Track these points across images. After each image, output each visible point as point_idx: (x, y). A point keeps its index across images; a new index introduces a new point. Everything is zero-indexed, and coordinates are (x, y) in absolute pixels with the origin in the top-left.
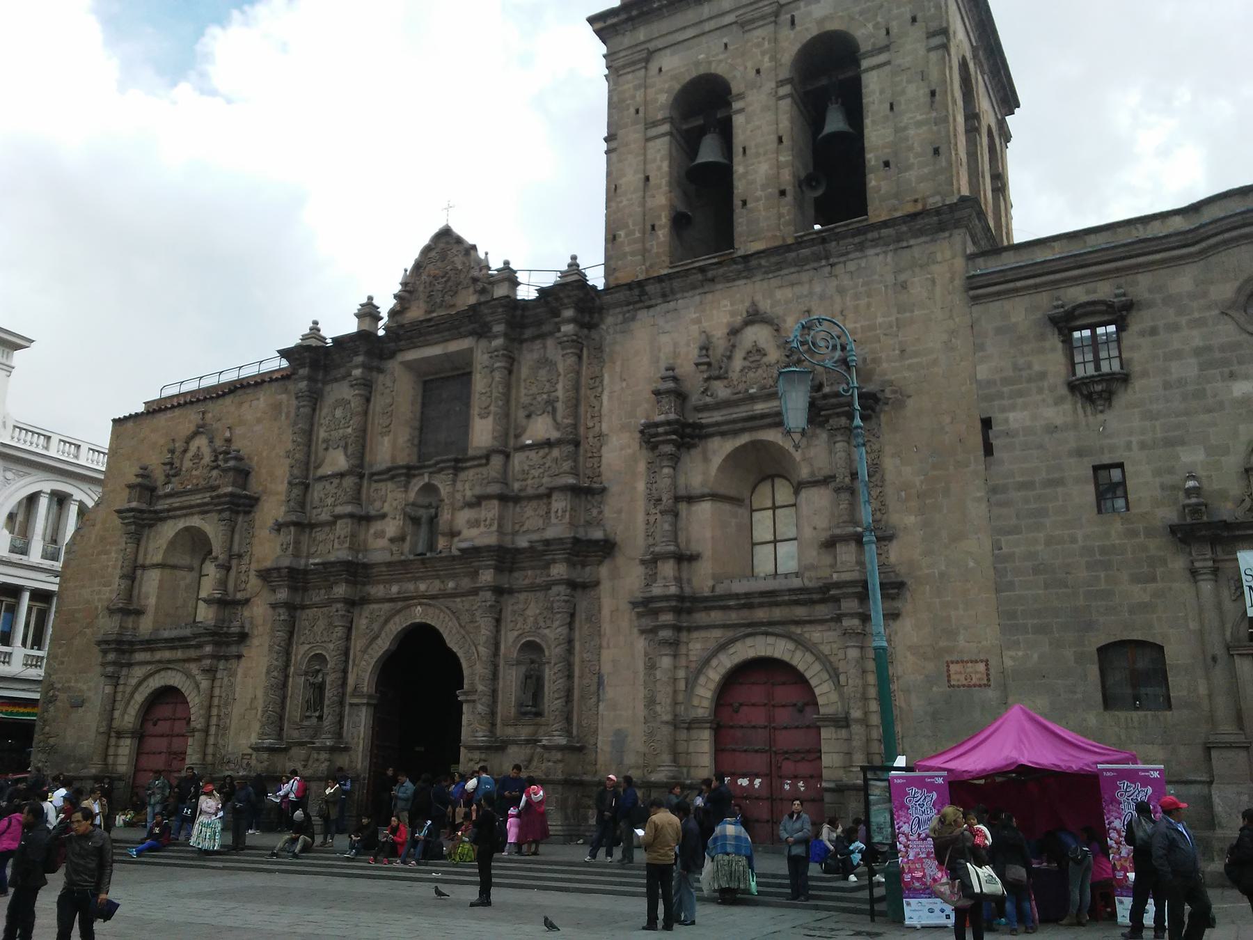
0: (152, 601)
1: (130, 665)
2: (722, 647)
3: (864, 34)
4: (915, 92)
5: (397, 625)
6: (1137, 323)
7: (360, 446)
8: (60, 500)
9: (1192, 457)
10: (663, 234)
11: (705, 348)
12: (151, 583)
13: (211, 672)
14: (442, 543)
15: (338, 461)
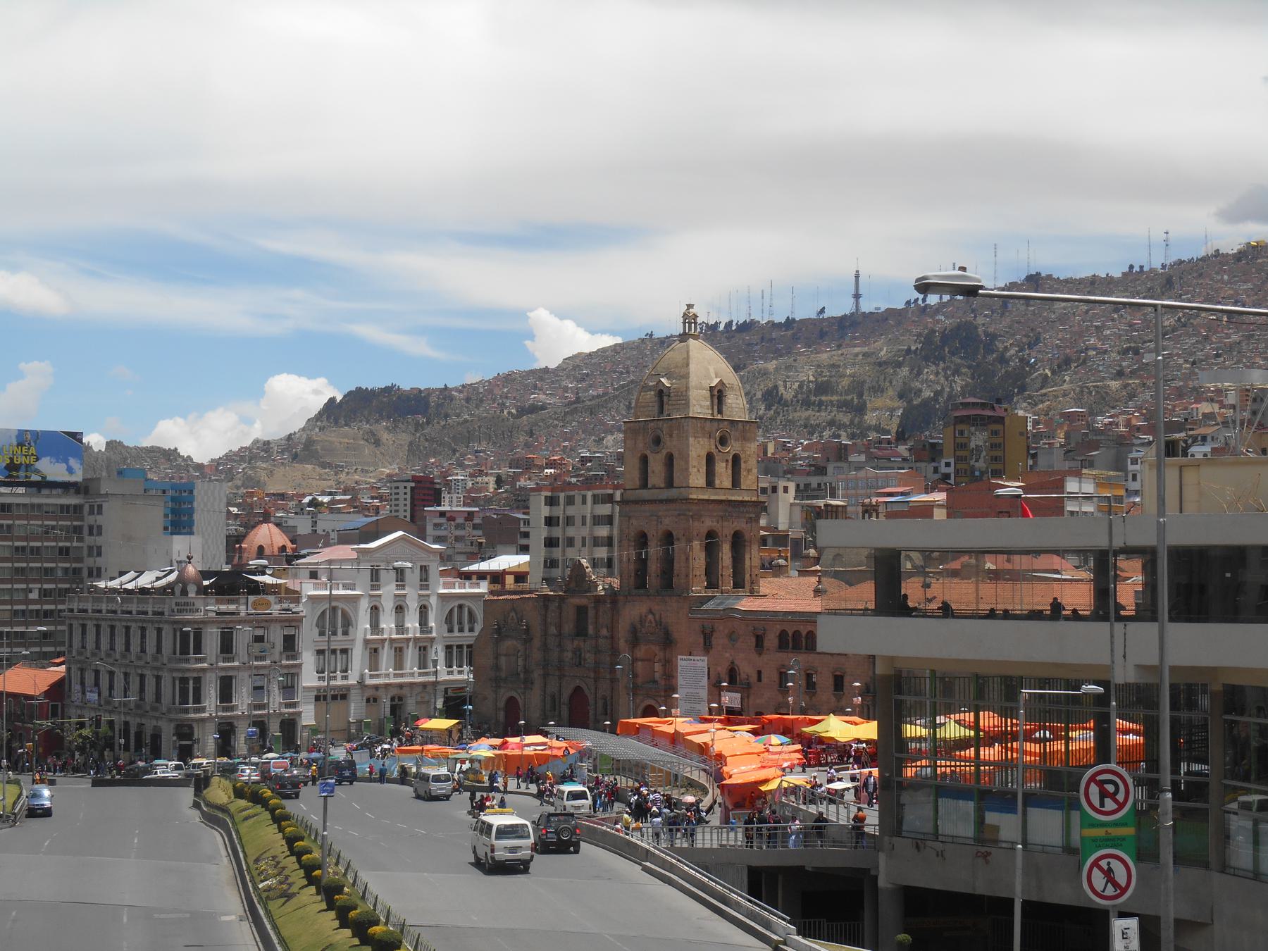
0: (504, 668)
1: (500, 687)
2: (642, 701)
3: (674, 533)
4: (683, 557)
5: (572, 686)
6: (715, 635)
7: (559, 627)
8: (460, 607)
9: (719, 669)
10: (632, 578)
11: (641, 617)
12: (503, 660)
13: (524, 693)
14: (582, 663)
15: (553, 630)
